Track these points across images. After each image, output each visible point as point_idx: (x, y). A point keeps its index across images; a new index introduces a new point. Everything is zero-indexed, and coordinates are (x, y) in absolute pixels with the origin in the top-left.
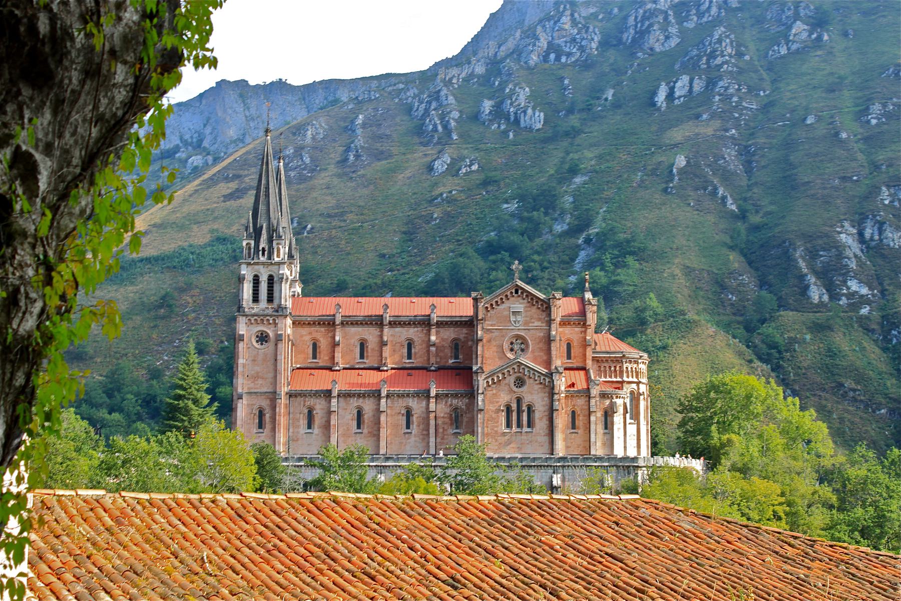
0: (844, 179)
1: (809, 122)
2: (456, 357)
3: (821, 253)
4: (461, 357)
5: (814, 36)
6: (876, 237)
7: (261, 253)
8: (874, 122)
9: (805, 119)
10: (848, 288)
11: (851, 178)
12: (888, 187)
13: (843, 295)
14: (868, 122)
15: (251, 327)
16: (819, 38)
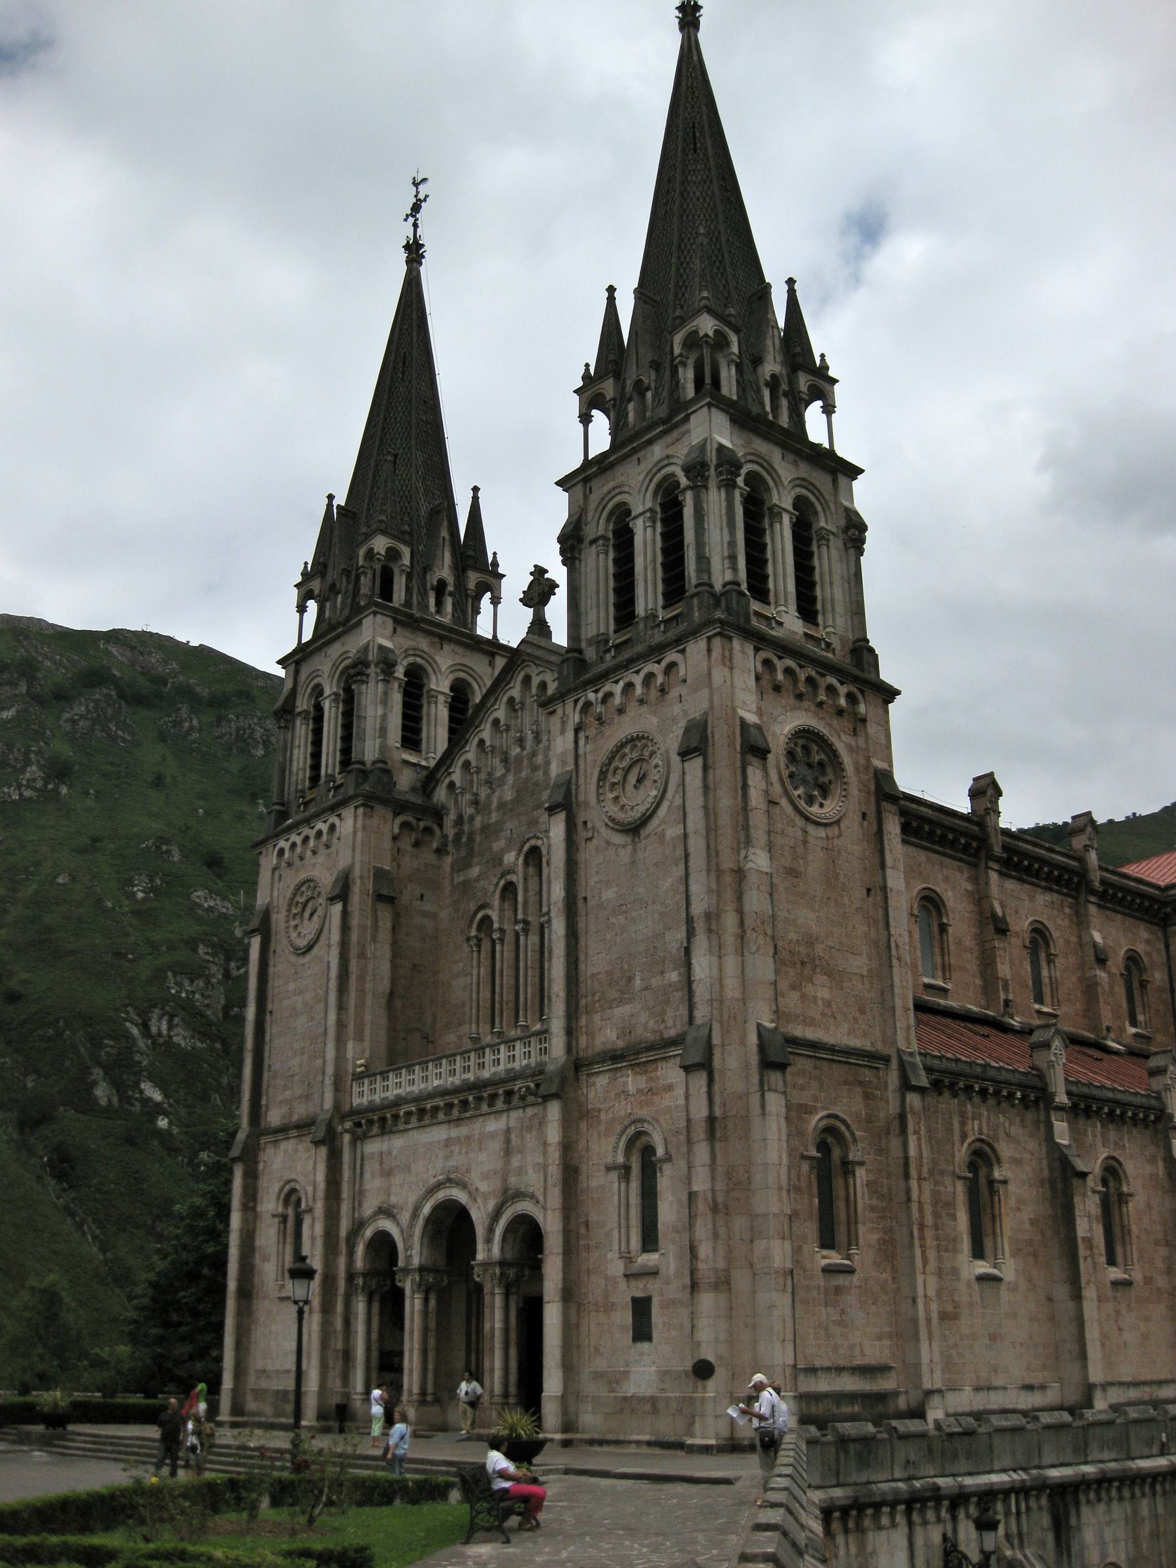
0: (118, 955)
1: (60, 880)
2: (1134, 1023)
3: (106, 1042)
4: (1141, 1018)
5: (50, 786)
6: (164, 1031)
7: (766, 393)
8: (140, 895)
9: (56, 877)
10: (141, 1092)
11: (125, 955)
12: (175, 973)
13: (137, 1099)
14: (134, 894)
15: (775, 703)
16: (56, 790)
